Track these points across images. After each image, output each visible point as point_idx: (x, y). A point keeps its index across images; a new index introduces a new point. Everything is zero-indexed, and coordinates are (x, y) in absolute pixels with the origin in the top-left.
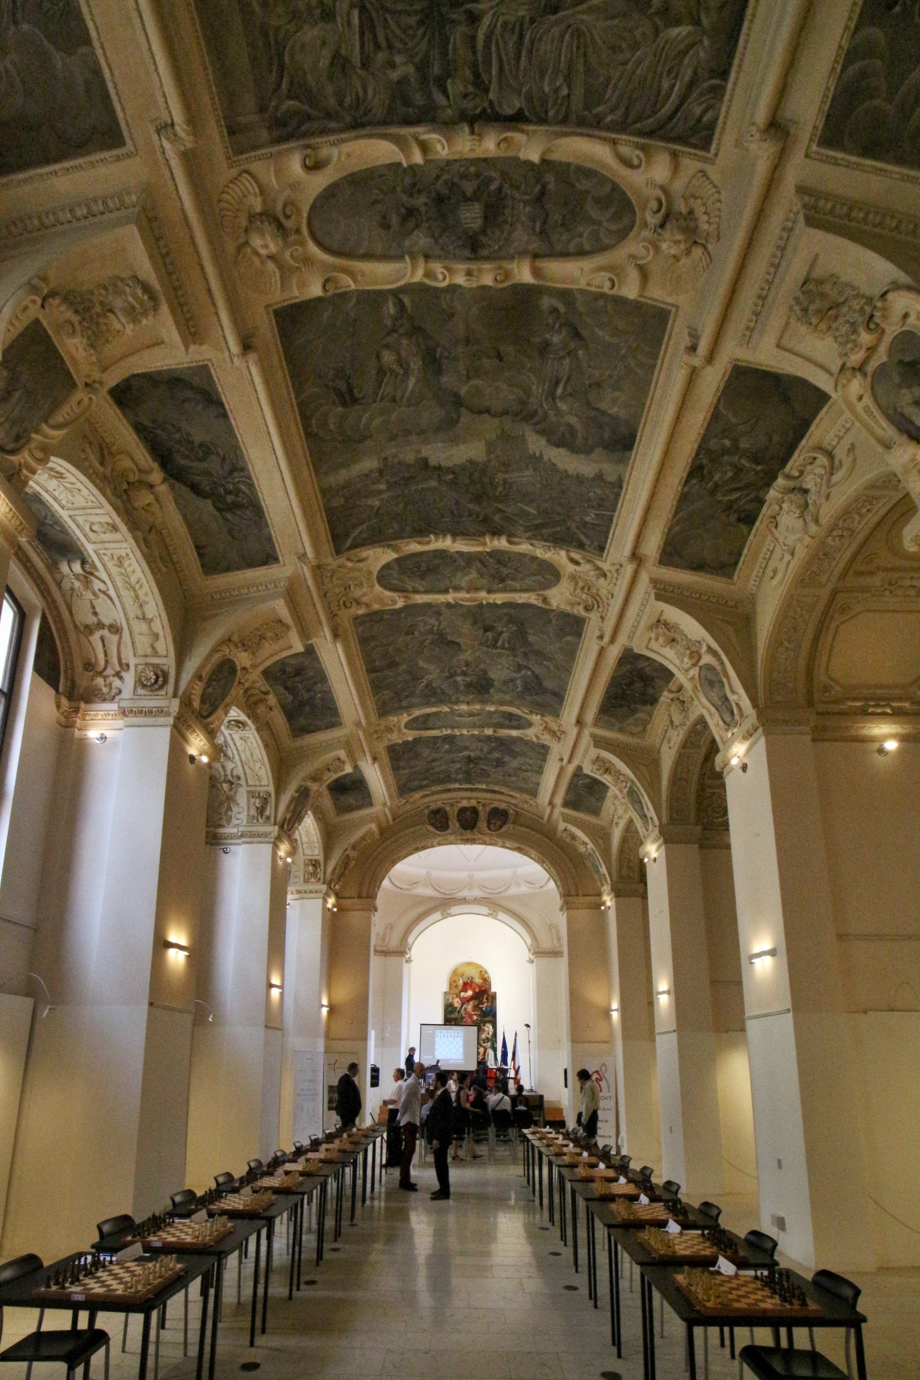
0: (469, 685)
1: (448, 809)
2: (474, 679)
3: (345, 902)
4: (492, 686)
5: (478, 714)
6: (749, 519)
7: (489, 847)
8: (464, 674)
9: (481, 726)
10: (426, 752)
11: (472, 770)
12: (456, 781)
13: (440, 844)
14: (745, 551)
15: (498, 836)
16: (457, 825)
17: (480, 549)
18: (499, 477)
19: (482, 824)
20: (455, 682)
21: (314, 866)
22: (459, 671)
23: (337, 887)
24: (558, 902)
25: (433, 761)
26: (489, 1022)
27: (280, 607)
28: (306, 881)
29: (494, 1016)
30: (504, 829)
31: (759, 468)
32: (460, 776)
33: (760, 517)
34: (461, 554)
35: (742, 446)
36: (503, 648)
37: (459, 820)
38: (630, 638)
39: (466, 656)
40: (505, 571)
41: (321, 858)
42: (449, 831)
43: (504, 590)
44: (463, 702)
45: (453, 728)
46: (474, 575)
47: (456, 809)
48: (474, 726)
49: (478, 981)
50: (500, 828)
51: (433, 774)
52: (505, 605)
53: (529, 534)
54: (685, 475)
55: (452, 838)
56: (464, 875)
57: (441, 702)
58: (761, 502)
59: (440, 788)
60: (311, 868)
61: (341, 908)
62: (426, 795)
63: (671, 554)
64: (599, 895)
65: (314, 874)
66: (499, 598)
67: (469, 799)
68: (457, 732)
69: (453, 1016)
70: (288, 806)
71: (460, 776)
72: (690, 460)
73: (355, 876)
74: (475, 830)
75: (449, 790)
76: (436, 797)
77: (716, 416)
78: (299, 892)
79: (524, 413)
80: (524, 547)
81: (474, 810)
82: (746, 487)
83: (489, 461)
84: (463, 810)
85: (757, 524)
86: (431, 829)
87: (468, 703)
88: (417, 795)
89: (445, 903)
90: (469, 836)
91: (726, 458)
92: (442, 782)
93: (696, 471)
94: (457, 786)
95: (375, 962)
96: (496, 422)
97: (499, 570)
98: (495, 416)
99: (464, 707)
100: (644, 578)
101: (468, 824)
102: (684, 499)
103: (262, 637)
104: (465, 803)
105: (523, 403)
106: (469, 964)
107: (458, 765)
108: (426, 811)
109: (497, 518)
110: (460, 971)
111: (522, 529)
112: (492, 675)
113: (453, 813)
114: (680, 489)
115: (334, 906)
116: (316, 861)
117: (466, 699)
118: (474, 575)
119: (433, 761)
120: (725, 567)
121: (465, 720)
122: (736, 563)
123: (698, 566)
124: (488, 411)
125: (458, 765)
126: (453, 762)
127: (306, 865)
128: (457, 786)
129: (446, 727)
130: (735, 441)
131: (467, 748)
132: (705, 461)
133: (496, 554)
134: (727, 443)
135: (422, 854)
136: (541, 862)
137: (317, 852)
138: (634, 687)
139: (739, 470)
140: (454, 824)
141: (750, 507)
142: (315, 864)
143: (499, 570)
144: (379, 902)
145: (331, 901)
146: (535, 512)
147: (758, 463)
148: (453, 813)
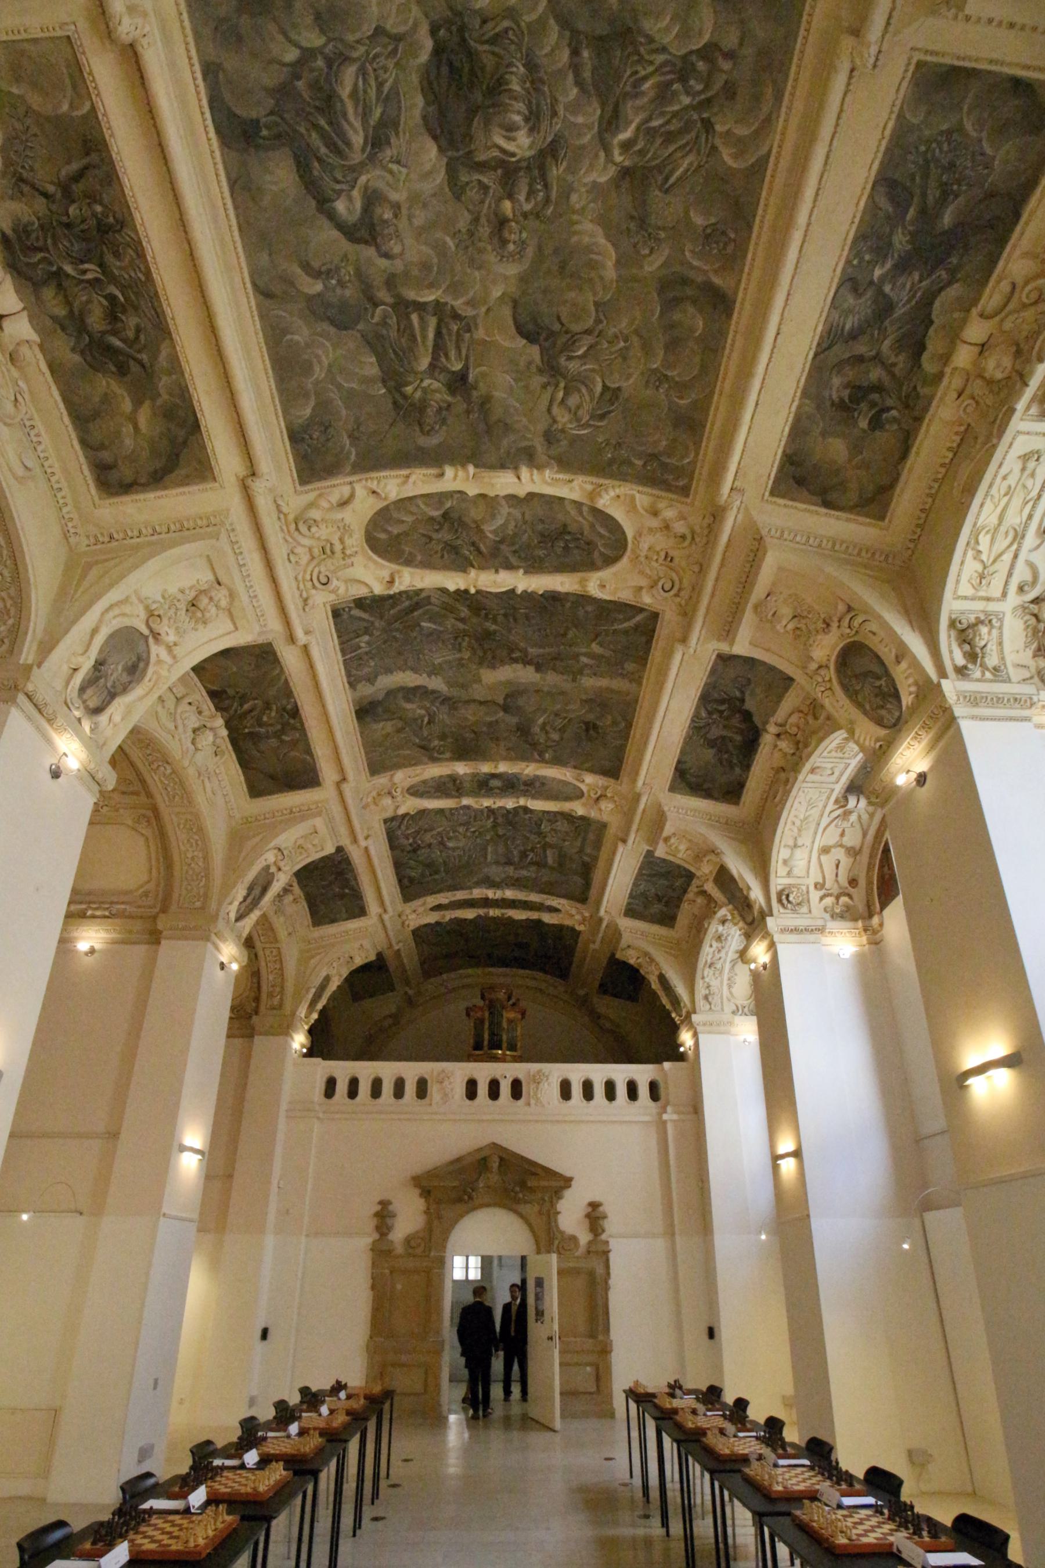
18: (467, 655)
34: (509, 567)
53: (423, 595)
109: (465, 612)
111: (433, 600)
146: (423, 624)
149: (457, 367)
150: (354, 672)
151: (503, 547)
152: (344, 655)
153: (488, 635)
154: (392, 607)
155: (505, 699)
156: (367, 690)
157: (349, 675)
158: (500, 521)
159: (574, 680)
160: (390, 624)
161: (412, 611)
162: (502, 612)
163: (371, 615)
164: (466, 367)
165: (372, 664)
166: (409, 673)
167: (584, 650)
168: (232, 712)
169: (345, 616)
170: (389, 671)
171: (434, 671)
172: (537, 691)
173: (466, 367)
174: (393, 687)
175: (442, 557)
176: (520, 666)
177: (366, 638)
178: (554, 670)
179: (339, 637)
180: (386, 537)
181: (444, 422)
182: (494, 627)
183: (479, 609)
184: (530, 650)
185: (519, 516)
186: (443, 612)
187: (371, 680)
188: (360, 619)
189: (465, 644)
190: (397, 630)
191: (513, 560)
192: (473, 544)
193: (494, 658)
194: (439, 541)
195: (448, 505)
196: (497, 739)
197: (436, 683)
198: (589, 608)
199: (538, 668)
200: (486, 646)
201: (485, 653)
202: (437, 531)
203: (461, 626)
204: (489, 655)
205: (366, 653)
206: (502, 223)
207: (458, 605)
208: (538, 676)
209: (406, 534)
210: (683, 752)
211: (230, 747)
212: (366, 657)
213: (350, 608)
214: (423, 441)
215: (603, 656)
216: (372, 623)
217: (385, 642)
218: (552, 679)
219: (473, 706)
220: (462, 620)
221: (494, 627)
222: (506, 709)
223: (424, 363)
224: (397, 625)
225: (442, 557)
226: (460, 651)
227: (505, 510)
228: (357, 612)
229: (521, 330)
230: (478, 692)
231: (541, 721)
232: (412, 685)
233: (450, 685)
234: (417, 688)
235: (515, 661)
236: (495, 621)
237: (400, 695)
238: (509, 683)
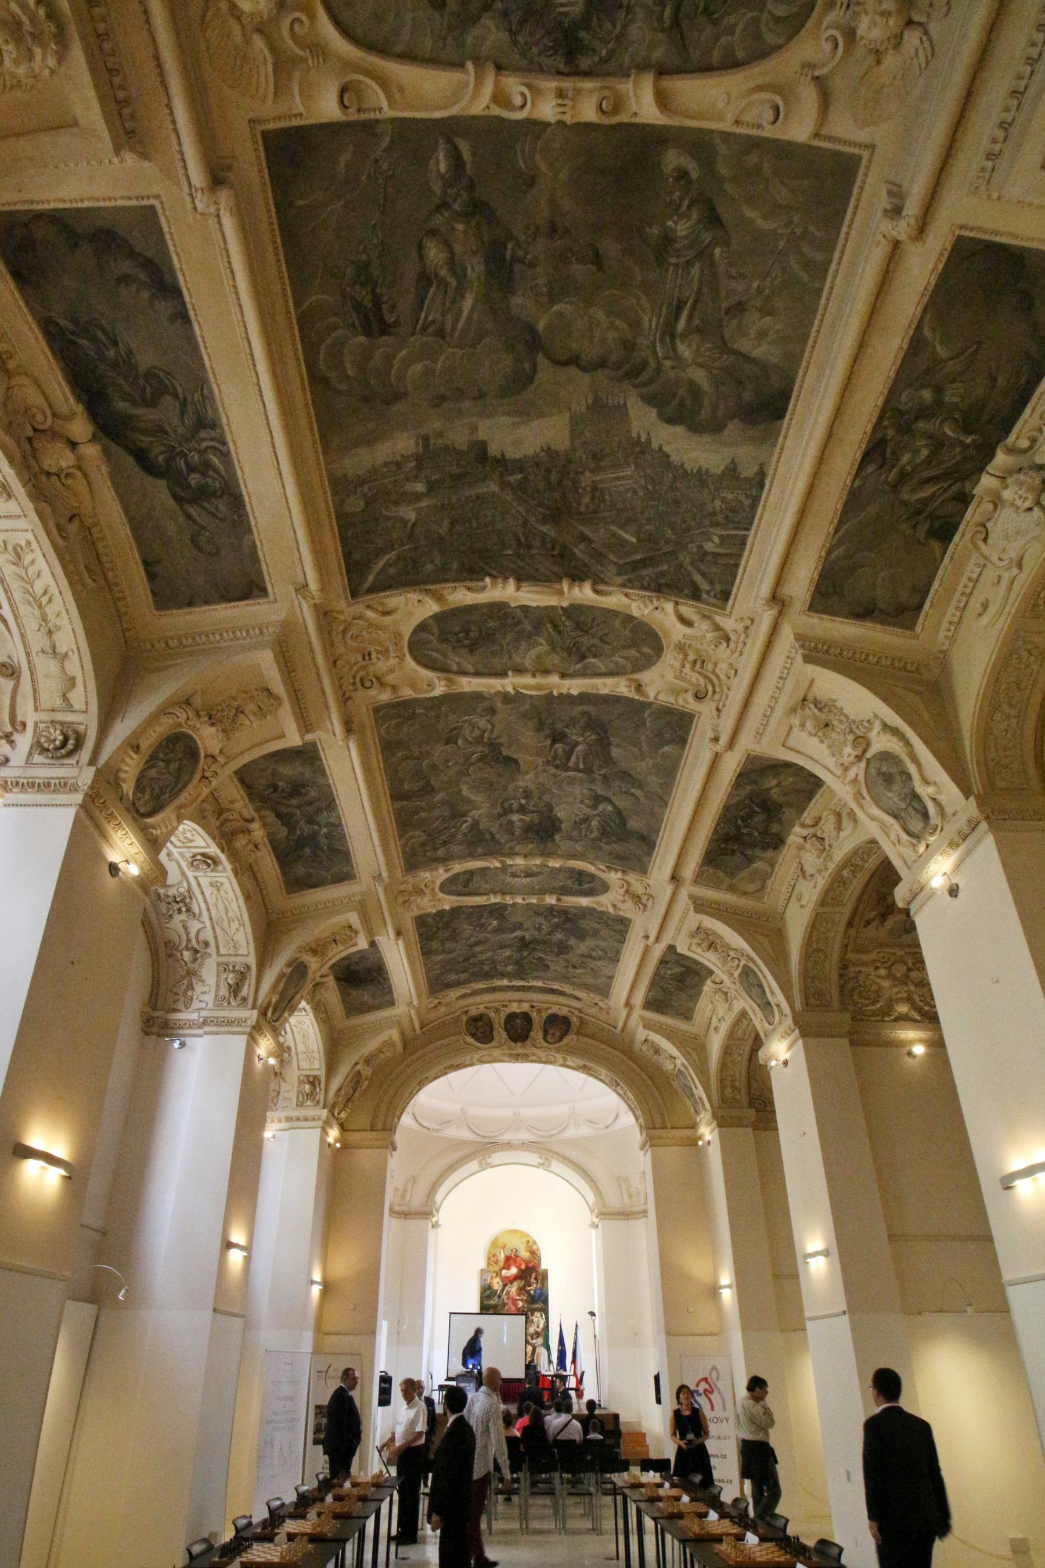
0: (527, 829)
1: (492, 1015)
2: (536, 817)
3: (354, 1137)
4: (559, 830)
5: (538, 874)
6: (945, 532)
7: (549, 1067)
8: (522, 809)
9: (542, 892)
10: (466, 929)
11: (528, 957)
12: (503, 975)
13: (482, 1062)
14: (936, 585)
15: (558, 1050)
16: (504, 1035)
17: (552, 601)
18: (587, 479)
19: (537, 1034)
20: (510, 823)
21: (312, 1083)
22: (515, 805)
23: (343, 1115)
24: (637, 1137)
25: (476, 944)
26: (538, 1310)
27: (266, 661)
28: (300, 1105)
29: (546, 1301)
30: (565, 1041)
31: (969, 440)
32: (509, 968)
33: (962, 527)
35: (947, 399)
36: (577, 769)
37: (506, 1030)
38: (759, 735)
39: (526, 781)
40: (585, 641)
41: (322, 1073)
42: (493, 1044)
43: (583, 674)
44: (517, 854)
45: (503, 893)
46: (542, 647)
47: (503, 1016)
48: (533, 893)
49: (524, 1254)
50: (561, 1039)
51: (475, 965)
52: (584, 698)
54: (859, 457)
55: (496, 1053)
56: (508, 1113)
57: (490, 854)
58: (964, 500)
59: (481, 985)
60: (307, 1087)
61: (346, 1146)
62: (464, 996)
63: (828, 595)
64: (694, 1126)
65: (311, 1095)
66: (575, 686)
67: (520, 1001)
68: (509, 900)
69: (492, 1302)
70: (275, 986)
71: (509, 968)
72: (869, 429)
73: (368, 1098)
74: (528, 1042)
75: (494, 990)
76: (477, 999)
77: (916, 345)
78: (289, 1119)
79: (630, 367)
80: (615, 600)
81: (526, 1017)
82: (947, 474)
83: (574, 449)
84: (511, 1017)
85: (956, 539)
86: (469, 1039)
87: (525, 856)
88: (453, 994)
89: (483, 1148)
90: (521, 1051)
91: (921, 425)
92: (487, 976)
93: (876, 451)
94: (505, 982)
95: (390, 1225)
96: (587, 378)
97: (579, 637)
98: (583, 369)
99: (520, 861)
100: (787, 633)
101: (520, 1034)
102: (853, 500)
103: (240, 711)
104: (515, 1008)
105: (628, 346)
106: (514, 1232)
107: (508, 953)
108: (464, 1018)
110: (501, 1241)
112: (561, 813)
113: (499, 1021)
114: (849, 483)
115: (336, 1141)
116: (315, 1077)
117: (524, 851)
118: (542, 647)
119: (476, 944)
120: (904, 613)
121: (520, 880)
122: (920, 606)
123: (865, 613)
124: (574, 361)
125: (508, 953)
126: (502, 947)
127: (301, 1082)
128: (505, 982)
129: (495, 893)
130: (939, 391)
131: (519, 926)
132: (890, 433)
133: (575, 611)
134: (927, 395)
135: (454, 1076)
136: (614, 1085)
137: (317, 1066)
138: (761, 812)
139: (938, 444)
140: (500, 1034)
141: (950, 508)
142: (313, 1081)
143: (579, 637)
144: (399, 1137)
145: (333, 1134)
147: (967, 432)
148: (499, 1021)
149: (559, 746)
150: (747, 502)
151: (529, 628)
152: (745, 537)
153: (556, 515)
154: (663, 574)
155: (534, 369)
156: (747, 457)
157: (755, 500)
158: (534, 652)
159: (426, 438)
160: (673, 553)
161: (642, 561)
162: (534, 552)
163: (689, 574)
164: (552, 745)
165: (718, 503)
166: (675, 458)
167: (424, 504)
168: (956, 488)
169: (718, 587)
170: (701, 477)
171: (639, 450)
172: (481, 395)
173: (552, 745)
174: (707, 438)
175: (593, 620)
176: (513, 453)
177: (709, 547)
178: (459, 452)
179: (737, 566)
180: (646, 644)
181: (572, 719)
182: (544, 529)
183: (562, 555)
184: (495, 488)
185: (514, 656)
186: (604, 551)
187: (732, 471)
188: (704, 575)
189: (586, 499)
190: (668, 541)
191: (519, 612)
192: (560, 633)
193: (549, 471)
194: (593, 637)
195: (578, 666)
196: (553, 230)
197: (643, 420)
198: (430, 567)
199: (480, 452)
200: (557, 495)
201: (560, 483)
202: (593, 645)
203: (587, 532)
204: (554, 477)
205: (717, 525)
206: (525, 798)
207: (586, 559)
208: (481, 435)
209: (624, 647)
210: (191, 340)
211: (1027, 411)
212: (720, 518)
213: (708, 593)
214: (592, 710)
215: (396, 503)
216: (692, 563)
217: (689, 529)
218: (459, 437)
219: (590, 352)
220: (584, 538)
221: (544, 529)
222: (532, 342)
223: (580, 748)
224: (667, 549)
225: (593, 620)
226: (595, 488)
227: (528, 662)
228: (705, 586)
229: (516, 762)
230: (579, 388)
231: (467, 304)
232: (680, 430)
233: (622, 410)
234: (670, 421)
235: (520, 465)
236: (543, 537)
237: (706, 413)
238: (525, 413)
